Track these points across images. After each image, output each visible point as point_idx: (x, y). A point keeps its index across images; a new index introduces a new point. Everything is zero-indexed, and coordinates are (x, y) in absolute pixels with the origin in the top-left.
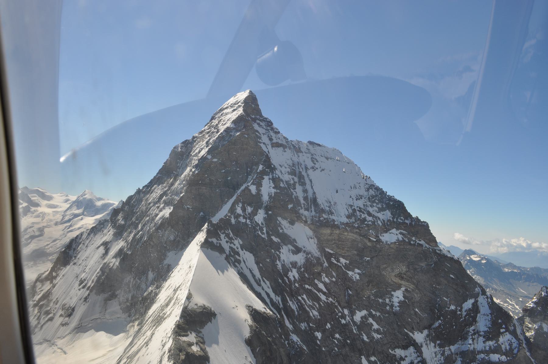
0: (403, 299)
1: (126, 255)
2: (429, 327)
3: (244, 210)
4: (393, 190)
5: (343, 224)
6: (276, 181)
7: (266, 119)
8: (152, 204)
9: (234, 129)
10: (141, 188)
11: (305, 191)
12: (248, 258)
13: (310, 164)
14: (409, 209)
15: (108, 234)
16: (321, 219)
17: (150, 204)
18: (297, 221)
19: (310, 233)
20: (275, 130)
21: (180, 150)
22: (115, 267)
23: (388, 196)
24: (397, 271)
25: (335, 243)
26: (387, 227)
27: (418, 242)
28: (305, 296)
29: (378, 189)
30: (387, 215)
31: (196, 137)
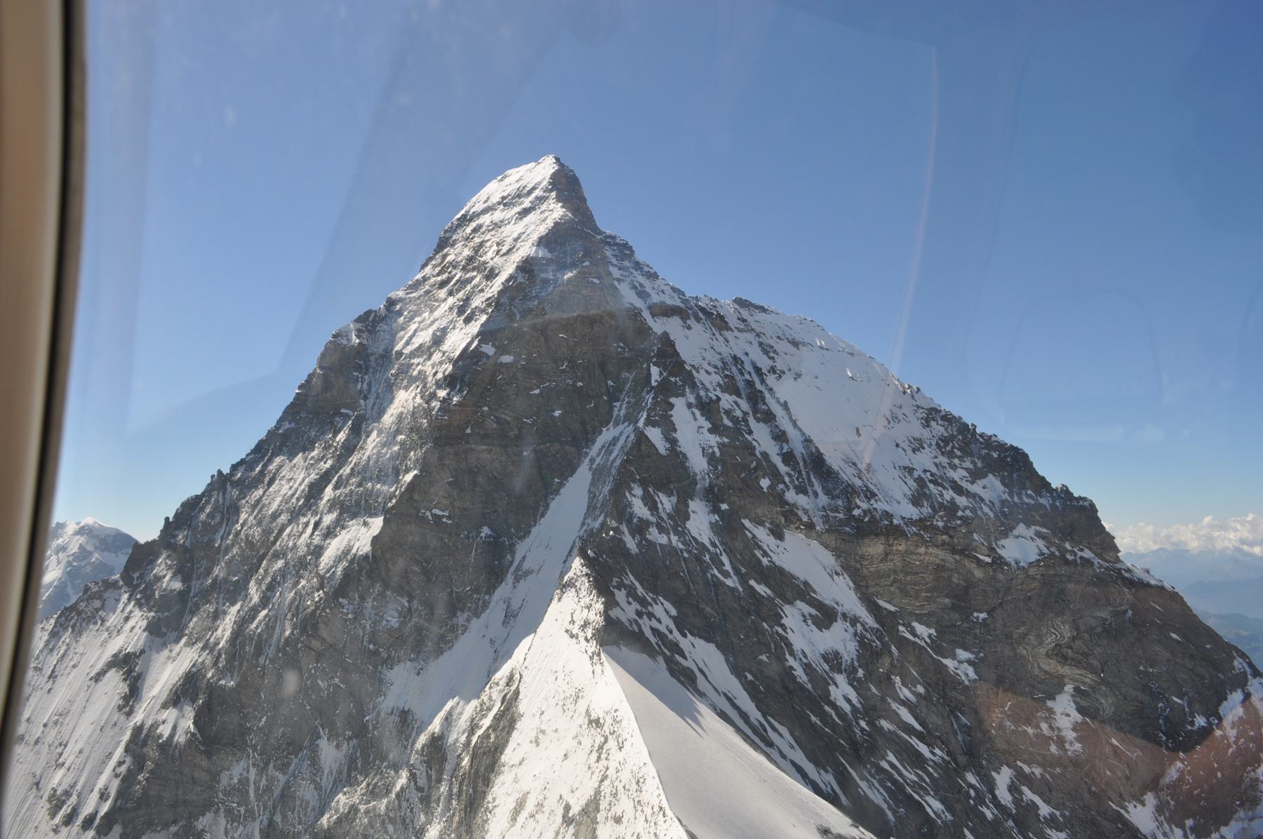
0: (1078, 717)
1: (213, 691)
2: (1153, 785)
4: (992, 421)
5: (910, 522)
7: (614, 238)
8: (283, 518)
9: (550, 261)
10: (226, 471)
11: (780, 437)
14: (1042, 468)
15: (127, 627)
16: (856, 512)
17: (275, 516)
18: (787, 527)
19: (829, 559)
20: (646, 269)
21: (355, 341)
22: (180, 738)
23: (982, 435)
24: (1050, 641)
25: (895, 581)
27: (1080, 554)
28: (891, 757)
29: (948, 419)
30: (991, 488)
31: (401, 300)
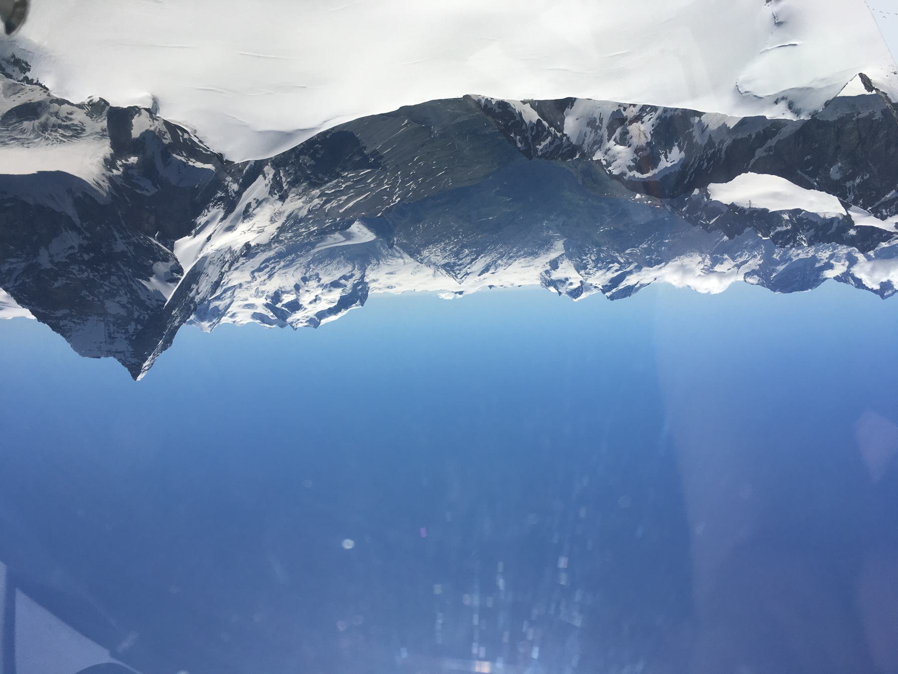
6: (127, 332)
12: (143, 297)
26: (64, 317)
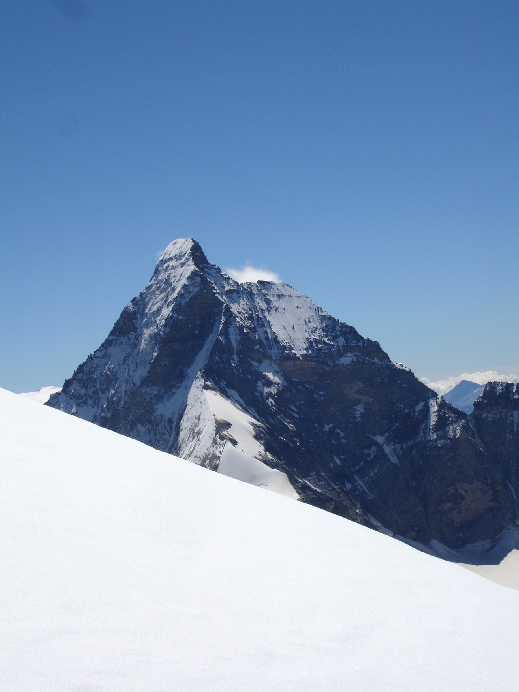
0: (363, 411)
3: (220, 357)
4: (343, 318)
10: (93, 353)
13: (264, 306)
16: (284, 354)
20: (225, 276)
29: (330, 318)
